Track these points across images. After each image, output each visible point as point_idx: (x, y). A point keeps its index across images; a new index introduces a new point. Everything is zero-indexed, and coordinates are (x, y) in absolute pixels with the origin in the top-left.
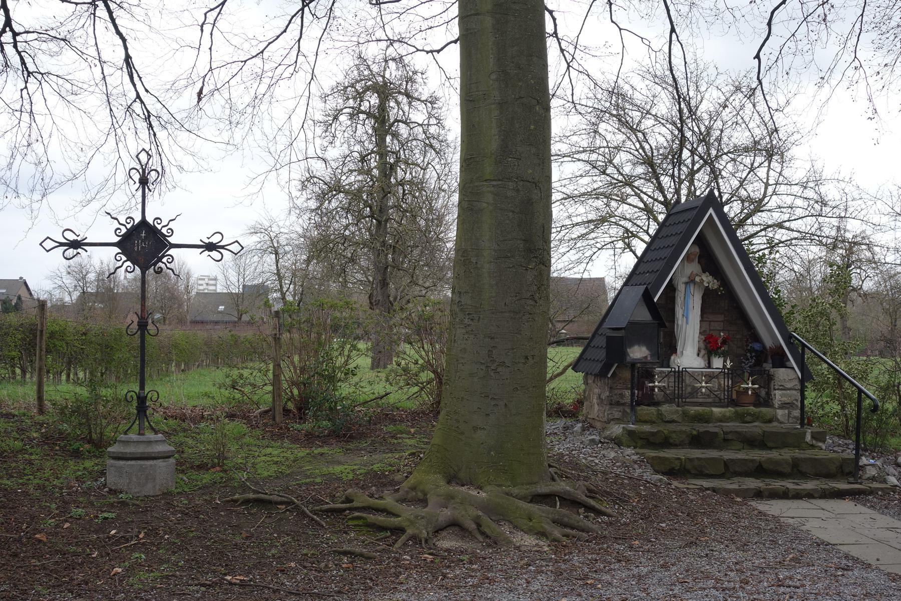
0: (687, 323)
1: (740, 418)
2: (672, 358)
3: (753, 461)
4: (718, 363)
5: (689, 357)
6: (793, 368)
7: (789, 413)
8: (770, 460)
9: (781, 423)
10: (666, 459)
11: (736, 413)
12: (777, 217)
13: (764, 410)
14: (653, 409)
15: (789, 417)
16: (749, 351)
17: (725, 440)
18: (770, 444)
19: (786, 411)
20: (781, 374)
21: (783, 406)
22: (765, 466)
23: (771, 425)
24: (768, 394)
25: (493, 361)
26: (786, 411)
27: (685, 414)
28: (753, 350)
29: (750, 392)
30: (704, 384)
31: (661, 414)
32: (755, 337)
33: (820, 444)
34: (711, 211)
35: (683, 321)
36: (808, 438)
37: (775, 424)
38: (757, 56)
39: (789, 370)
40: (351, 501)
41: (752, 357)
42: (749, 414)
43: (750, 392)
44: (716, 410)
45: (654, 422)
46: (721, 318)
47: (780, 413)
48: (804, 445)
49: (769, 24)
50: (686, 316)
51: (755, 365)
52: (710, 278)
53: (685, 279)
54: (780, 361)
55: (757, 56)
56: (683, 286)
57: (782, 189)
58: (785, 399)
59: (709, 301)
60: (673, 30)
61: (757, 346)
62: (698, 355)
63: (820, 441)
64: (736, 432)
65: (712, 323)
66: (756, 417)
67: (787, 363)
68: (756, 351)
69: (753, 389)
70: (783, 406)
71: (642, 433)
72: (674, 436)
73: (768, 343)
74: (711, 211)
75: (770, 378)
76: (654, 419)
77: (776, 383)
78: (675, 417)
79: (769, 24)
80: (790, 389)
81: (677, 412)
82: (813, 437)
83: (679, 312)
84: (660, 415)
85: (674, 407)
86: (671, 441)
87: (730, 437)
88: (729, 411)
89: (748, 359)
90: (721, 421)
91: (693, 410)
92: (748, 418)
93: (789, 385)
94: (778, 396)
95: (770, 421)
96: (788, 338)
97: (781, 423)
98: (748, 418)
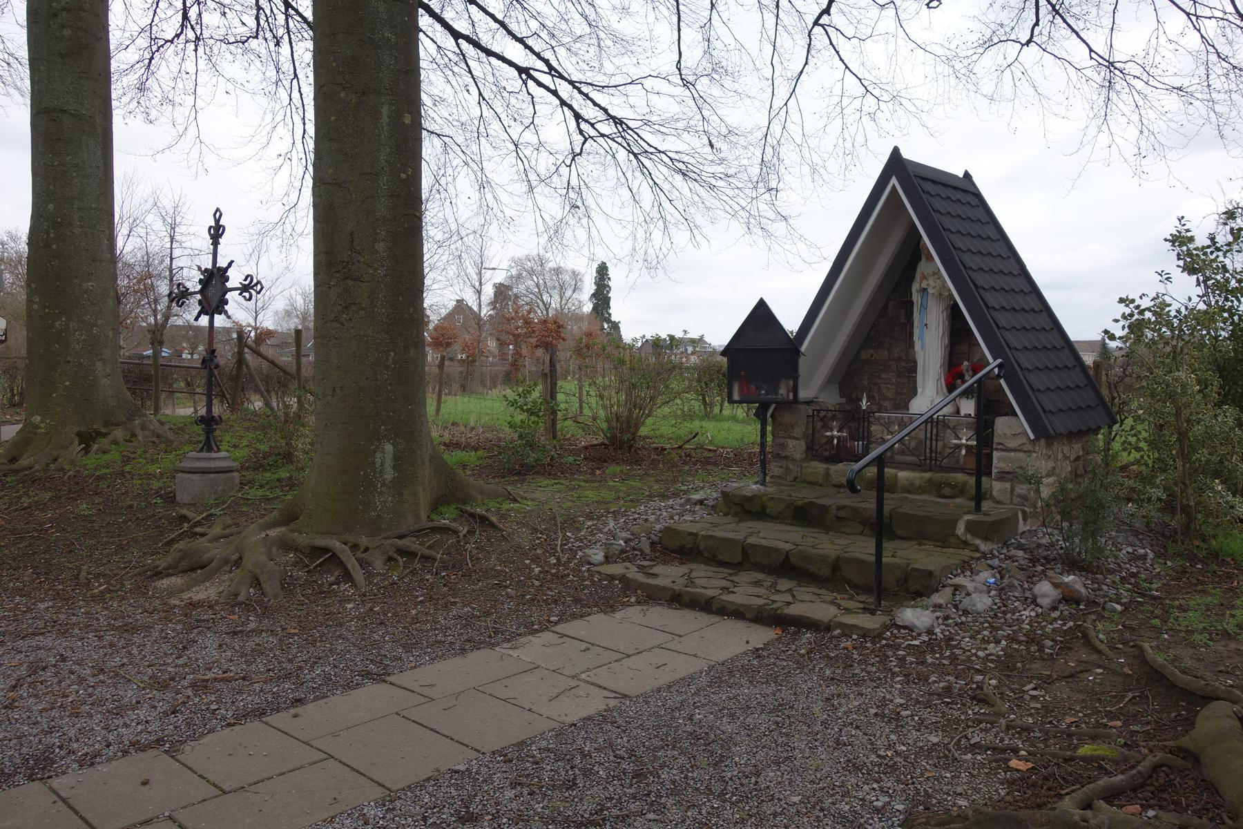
1: (936, 488)
3: (777, 550)
5: (928, 397)
7: (1012, 489)
11: (930, 480)
17: (839, 518)
18: (899, 532)
21: (1004, 476)
22: (793, 560)
26: (1008, 485)
33: (977, 541)
34: (894, 181)
36: (961, 529)
42: (949, 485)
48: (952, 540)
50: (921, 338)
63: (978, 536)
64: (852, 508)
69: (967, 446)
74: (894, 181)
80: (1015, 450)
82: (967, 529)
84: (827, 474)
87: (842, 514)
90: (908, 491)
92: (947, 491)
97: (999, 502)
98: (947, 491)
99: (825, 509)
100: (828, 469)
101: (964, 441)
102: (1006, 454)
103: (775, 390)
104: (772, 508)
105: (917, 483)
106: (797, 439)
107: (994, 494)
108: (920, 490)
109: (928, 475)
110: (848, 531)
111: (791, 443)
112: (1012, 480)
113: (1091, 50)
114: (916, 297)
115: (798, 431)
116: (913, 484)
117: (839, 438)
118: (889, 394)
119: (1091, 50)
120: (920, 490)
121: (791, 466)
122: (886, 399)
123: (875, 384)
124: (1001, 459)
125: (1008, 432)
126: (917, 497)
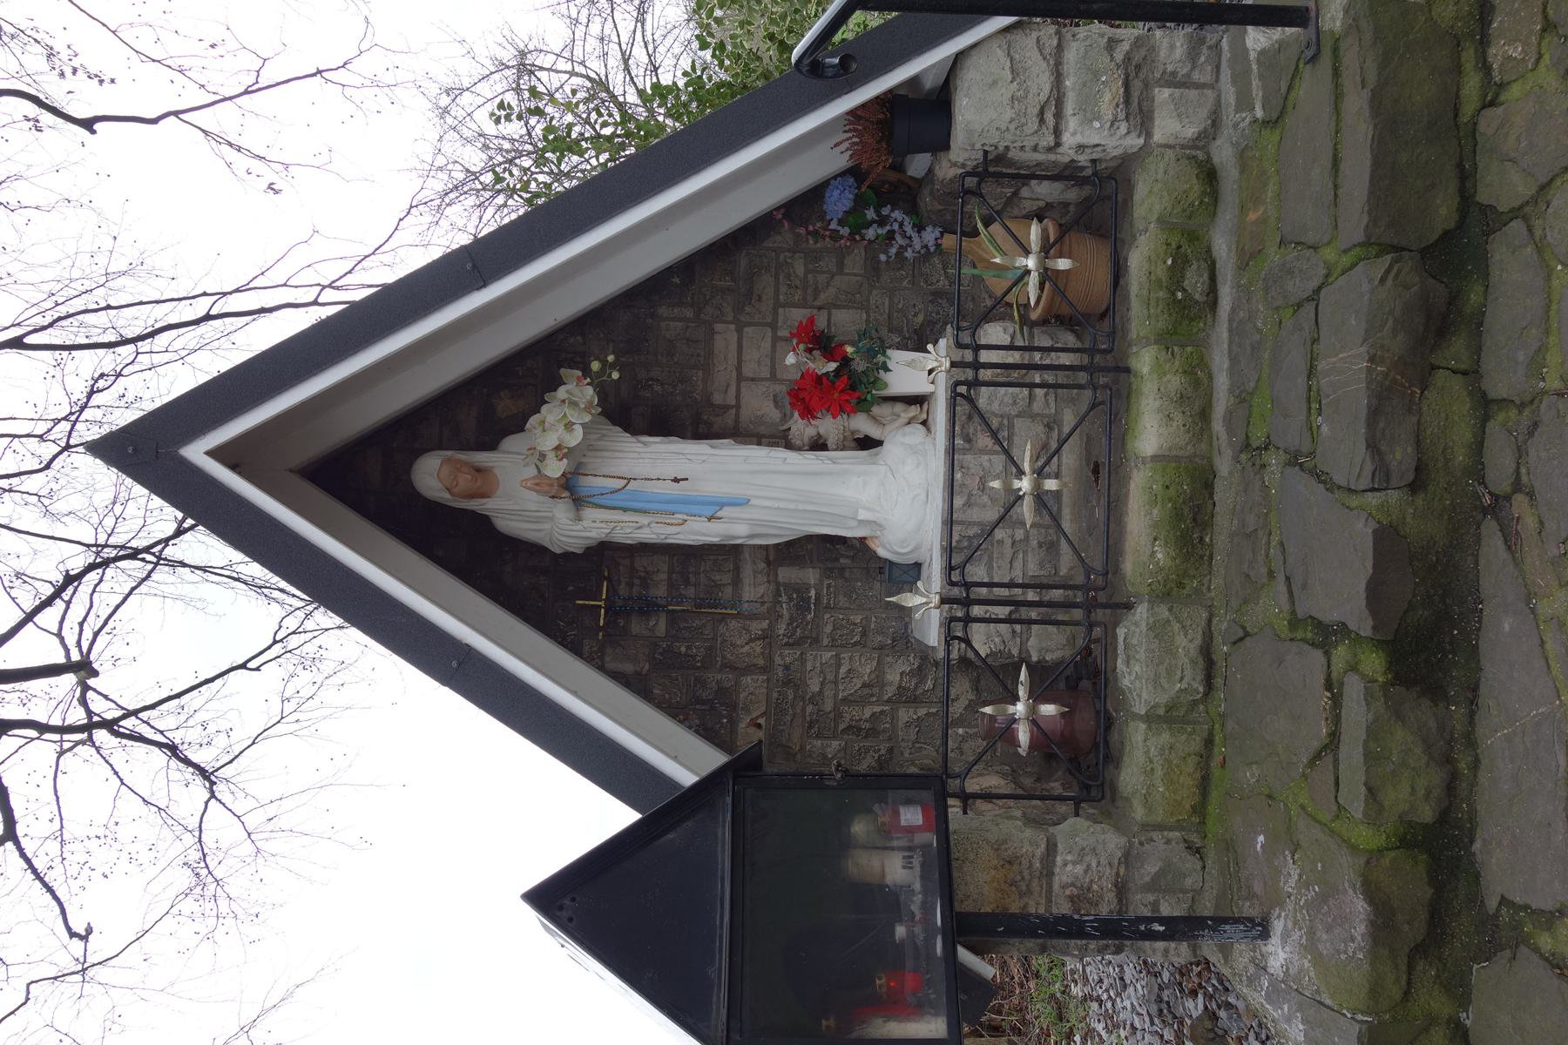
0: (743, 503)
1: (1188, 316)
2: (882, 552)
6: (959, 57)
7: (1172, 81)
9: (1215, 121)
11: (1166, 340)
12: (614, 61)
13: (1150, 199)
15: (1185, 84)
16: (858, 228)
17: (1415, 486)
19: (1163, 95)
20: (983, 116)
21: (1138, 112)
23: (1230, 175)
24: (1067, 174)
26: (1163, 95)
27: (1169, 592)
28: (854, 220)
29: (1063, 264)
30: (1025, 485)
31: (1170, 708)
32: (805, 205)
34: (197, 452)
35: (733, 520)
37: (1223, 153)
38: (88, 124)
39: (970, 78)
41: (882, 221)
43: (1063, 264)
44: (1151, 432)
45: (1209, 742)
46: (725, 339)
47: (1170, 126)
50: (714, 508)
51: (913, 209)
52: (550, 413)
53: (561, 512)
54: (924, 113)
55: (88, 124)
56: (590, 513)
58: (1109, 98)
59: (660, 404)
61: (839, 202)
62: (867, 443)
64: (1374, 414)
65: (748, 371)
66: (1188, 246)
67: (929, 83)
68: (860, 203)
69: (1046, 249)
70: (1138, 112)
71: (1375, 991)
72: (1398, 797)
73: (832, 160)
74: (197, 452)
75: (996, 168)
76: (1196, 744)
77: (1028, 145)
78: (1186, 645)
81: (1158, 630)
84: (1167, 717)
85: (1134, 630)
86: (1427, 814)
87: (1401, 456)
89: (890, 236)
90: (1204, 415)
91: (1144, 541)
92: (1195, 282)
93: (1041, 82)
94: (1091, 133)
95: (1210, 175)
96: (823, 72)
97: (1215, 121)
98: (1195, 282)
99: (1387, 539)
100: (1149, 718)
101: (1031, 262)
102: (1069, 107)
103: (888, 901)
104: (1411, 795)
105: (1175, 382)
106: (1051, 848)
107: (1190, 132)
108: (1197, 376)
109: (1144, 361)
110: (1462, 434)
111: (1068, 870)
112: (1147, 86)
113: (243, 666)
114: (593, 527)
115: (1026, 841)
116: (1182, 398)
117: (1037, 696)
118: (867, 670)
119: (243, 666)
120: (1197, 376)
121: (1151, 868)
122: (878, 680)
123: (839, 716)
124: (1089, 115)
125: (1006, 91)
126: (1222, 382)
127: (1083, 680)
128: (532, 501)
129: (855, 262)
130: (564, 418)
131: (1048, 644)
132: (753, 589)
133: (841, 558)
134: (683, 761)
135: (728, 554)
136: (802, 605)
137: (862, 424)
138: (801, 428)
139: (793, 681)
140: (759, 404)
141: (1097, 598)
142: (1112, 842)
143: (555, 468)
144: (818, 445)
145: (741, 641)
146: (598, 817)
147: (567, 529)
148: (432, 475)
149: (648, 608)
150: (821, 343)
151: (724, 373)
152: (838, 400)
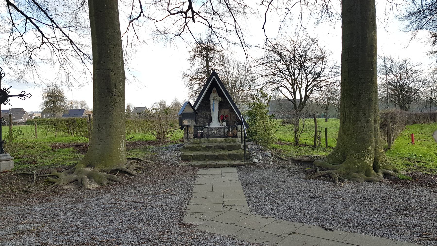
3: (214, 155)
4: (224, 124)
5: (215, 123)
8: (220, 155)
10: (186, 155)
12: (323, 78)
14: (198, 139)
25: (100, 128)
34: (214, 76)
40: (51, 173)
46: (228, 110)
49: (265, 17)
50: (213, 110)
53: (212, 99)
57: (325, 70)
60: (235, 21)
62: (219, 122)
74: (214, 76)
79: (265, 17)
81: (206, 140)
83: (211, 109)
84: (200, 141)
85: (206, 138)
88: (223, 139)
127: (202, 136)
128: (213, 96)
129: (234, 120)
130: (219, 99)
131: (205, 134)
132: (207, 113)
133: (210, 121)
134: (196, 109)
135: (210, 111)
136: (206, 117)
137: (221, 121)
138: (220, 116)
139: (200, 117)
140: (222, 113)
141: (208, 136)
142: (192, 137)
143: (215, 98)
144: (219, 118)
145: (203, 113)
146: (193, 104)
147: (211, 99)
148: (214, 89)
149: (206, 105)
150: (226, 117)
151: (225, 110)
152: (222, 118)
